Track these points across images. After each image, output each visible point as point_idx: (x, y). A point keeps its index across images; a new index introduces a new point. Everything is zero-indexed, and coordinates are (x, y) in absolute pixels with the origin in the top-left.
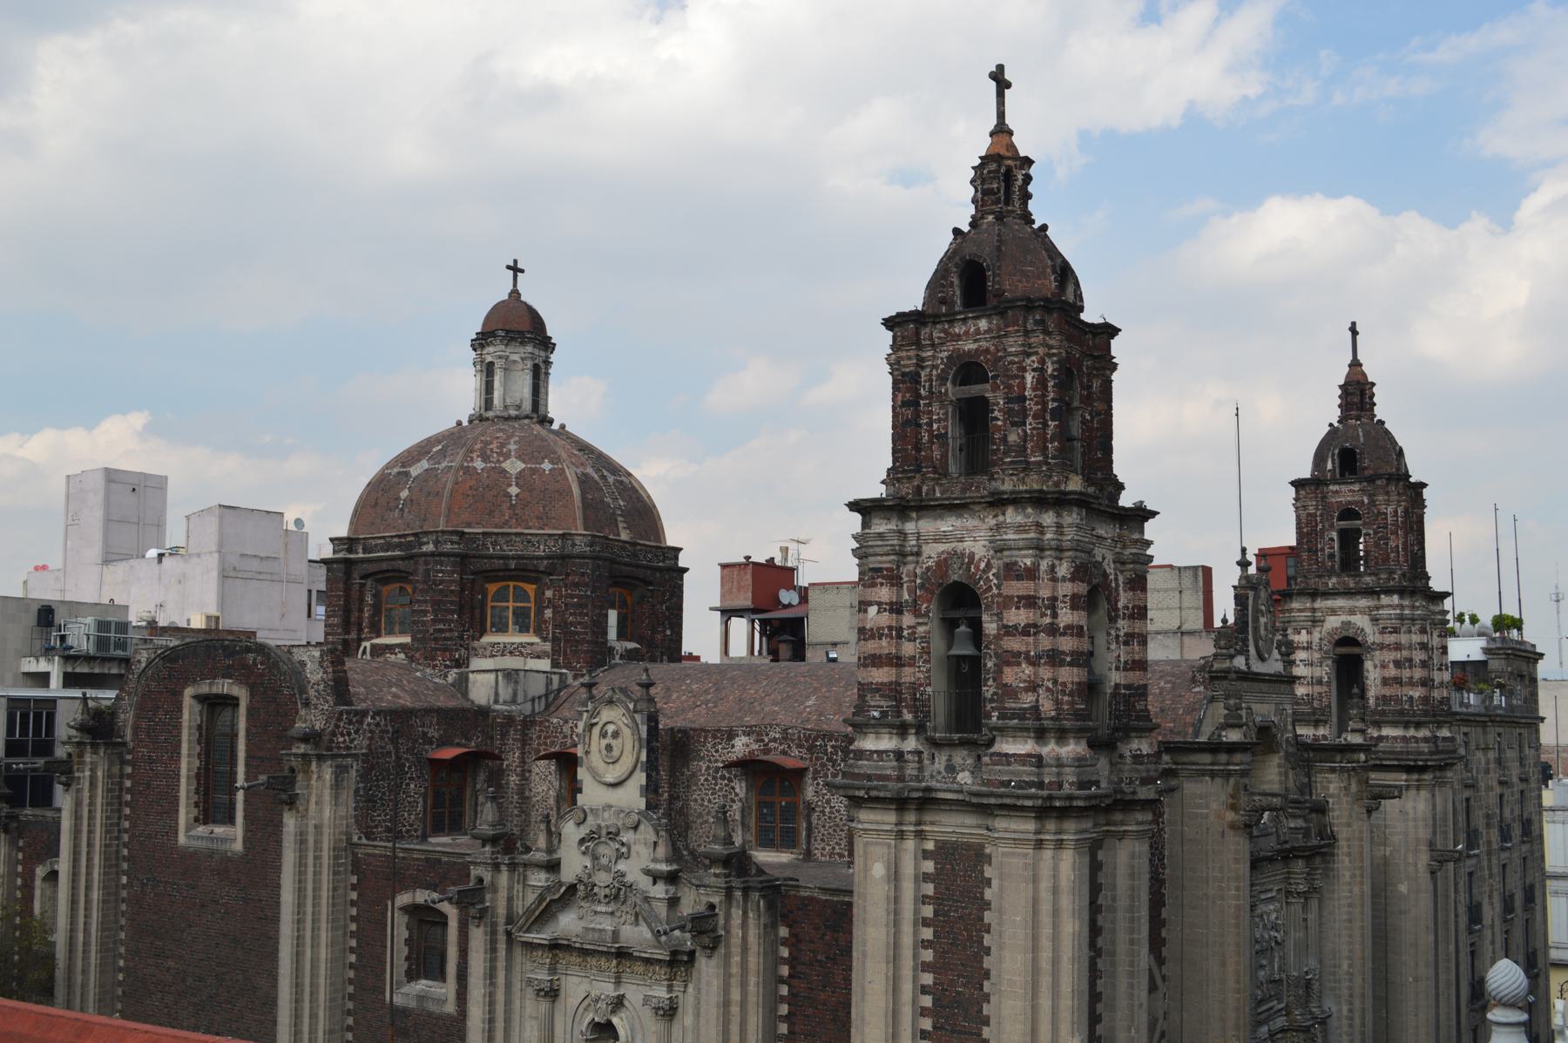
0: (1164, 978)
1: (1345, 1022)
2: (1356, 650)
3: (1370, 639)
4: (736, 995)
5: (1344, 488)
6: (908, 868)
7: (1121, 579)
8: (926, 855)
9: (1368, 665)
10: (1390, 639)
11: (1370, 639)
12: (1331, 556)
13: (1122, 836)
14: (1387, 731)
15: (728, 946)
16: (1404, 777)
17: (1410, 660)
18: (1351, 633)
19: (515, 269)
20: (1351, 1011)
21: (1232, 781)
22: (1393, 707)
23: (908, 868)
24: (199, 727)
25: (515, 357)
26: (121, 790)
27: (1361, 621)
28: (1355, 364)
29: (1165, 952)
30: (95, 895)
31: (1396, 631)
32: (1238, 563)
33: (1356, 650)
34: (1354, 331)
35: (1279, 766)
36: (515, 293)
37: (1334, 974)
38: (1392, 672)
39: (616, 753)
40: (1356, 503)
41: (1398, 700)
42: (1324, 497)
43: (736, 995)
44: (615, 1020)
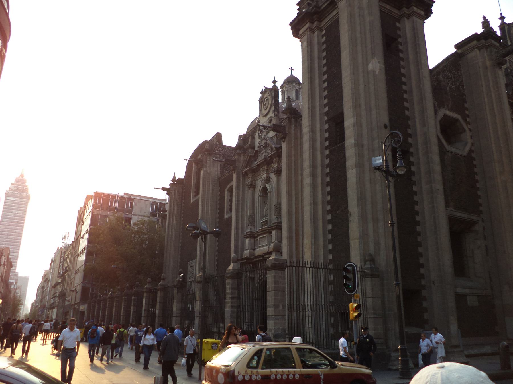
0: (470, 130)
4: (293, 153)
13: (409, 17)
19: (291, 69)
21: (489, 50)
24: (196, 172)
25: (291, 88)
29: (468, 120)
32: (500, 19)
36: (292, 74)
39: (267, 104)
43: (293, 153)
44: (267, 185)
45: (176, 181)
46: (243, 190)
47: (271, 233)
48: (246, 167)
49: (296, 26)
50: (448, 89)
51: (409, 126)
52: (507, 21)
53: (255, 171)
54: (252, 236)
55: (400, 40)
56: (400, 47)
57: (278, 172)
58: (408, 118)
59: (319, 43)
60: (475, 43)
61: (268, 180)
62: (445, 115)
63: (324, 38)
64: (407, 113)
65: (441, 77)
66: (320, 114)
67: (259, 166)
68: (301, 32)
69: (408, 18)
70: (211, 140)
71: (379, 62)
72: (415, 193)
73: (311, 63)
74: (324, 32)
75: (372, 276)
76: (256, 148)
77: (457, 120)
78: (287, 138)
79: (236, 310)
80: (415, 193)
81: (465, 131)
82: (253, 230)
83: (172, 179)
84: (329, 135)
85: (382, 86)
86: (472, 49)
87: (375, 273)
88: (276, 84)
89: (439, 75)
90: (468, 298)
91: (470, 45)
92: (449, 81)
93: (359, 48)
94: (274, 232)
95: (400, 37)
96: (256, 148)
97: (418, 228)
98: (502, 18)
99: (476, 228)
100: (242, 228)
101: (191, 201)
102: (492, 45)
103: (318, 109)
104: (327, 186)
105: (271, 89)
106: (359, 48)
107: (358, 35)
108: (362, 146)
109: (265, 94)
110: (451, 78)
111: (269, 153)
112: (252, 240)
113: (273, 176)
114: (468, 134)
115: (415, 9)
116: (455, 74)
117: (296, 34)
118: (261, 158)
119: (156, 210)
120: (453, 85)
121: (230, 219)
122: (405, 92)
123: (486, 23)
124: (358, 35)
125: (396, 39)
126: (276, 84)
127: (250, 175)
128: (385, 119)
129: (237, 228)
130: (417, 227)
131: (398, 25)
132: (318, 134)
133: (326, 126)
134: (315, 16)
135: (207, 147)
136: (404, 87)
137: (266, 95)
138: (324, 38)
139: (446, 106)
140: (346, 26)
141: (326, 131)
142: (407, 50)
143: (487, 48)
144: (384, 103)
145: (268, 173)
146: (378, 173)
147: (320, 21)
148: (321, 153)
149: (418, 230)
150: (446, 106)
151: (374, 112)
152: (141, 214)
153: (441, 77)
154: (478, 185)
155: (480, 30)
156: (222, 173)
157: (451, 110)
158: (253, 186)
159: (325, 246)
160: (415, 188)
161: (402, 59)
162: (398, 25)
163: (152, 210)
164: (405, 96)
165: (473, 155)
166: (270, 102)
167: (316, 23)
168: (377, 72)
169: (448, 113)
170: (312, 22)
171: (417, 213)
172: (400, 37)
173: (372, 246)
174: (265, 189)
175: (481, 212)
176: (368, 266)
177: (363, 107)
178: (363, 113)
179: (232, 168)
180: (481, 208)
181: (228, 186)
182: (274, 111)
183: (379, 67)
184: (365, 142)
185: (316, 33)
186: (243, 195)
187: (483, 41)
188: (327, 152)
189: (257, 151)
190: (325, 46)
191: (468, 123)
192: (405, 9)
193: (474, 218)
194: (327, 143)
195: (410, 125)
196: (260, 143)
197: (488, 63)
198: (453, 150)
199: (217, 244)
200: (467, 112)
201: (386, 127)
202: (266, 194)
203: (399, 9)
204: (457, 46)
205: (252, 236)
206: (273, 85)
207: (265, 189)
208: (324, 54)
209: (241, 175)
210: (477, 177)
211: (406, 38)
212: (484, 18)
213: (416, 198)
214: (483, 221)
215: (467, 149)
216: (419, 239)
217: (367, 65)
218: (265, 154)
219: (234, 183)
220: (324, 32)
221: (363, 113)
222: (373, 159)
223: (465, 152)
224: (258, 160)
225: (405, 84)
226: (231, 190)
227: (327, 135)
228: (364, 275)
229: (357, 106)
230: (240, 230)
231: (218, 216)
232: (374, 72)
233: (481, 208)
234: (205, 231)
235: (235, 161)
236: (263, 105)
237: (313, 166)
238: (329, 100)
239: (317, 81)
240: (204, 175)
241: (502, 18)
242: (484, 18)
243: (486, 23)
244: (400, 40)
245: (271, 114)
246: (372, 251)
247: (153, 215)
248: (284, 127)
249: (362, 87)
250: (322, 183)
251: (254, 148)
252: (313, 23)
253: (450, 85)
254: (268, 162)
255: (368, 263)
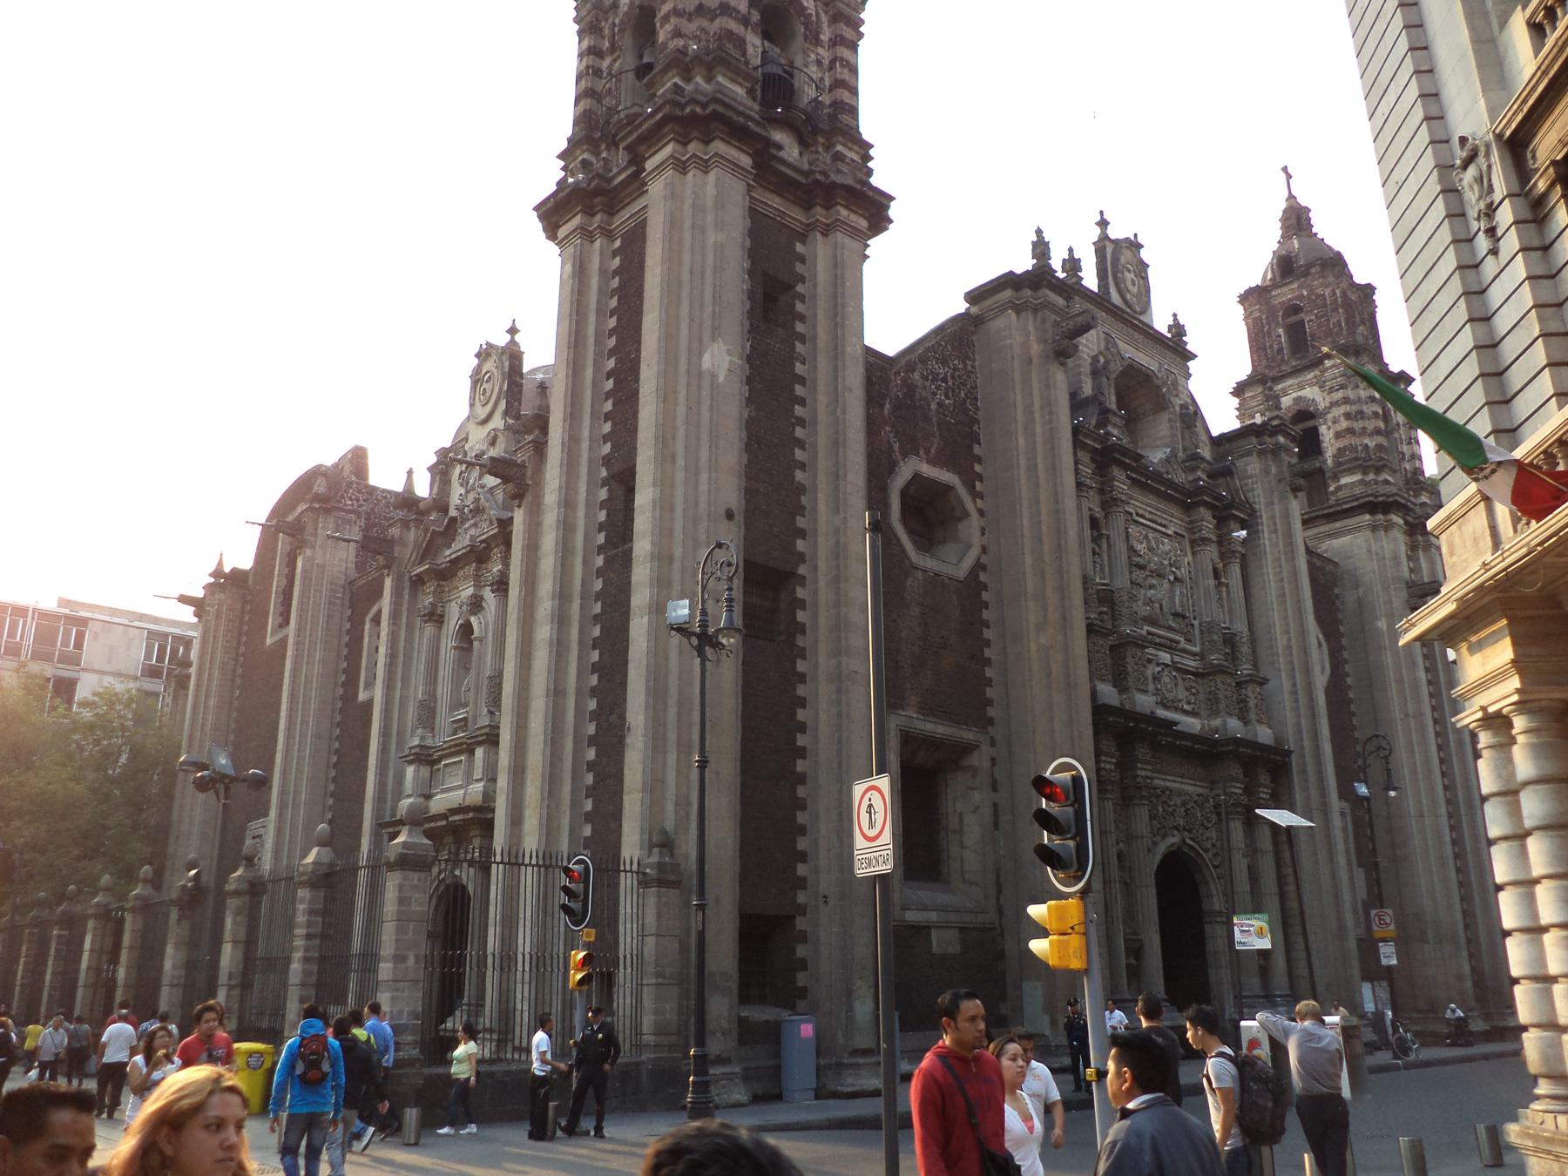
0: (981, 513)
1: (1286, 696)
2: (1309, 424)
3: (1322, 406)
5: (1285, 289)
6: (595, 264)
7: (824, 18)
8: (614, 254)
9: (1323, 429)
10: (1339, 395)
11: (1322, 406)
12: (1280, 350)
13: (827, 231)
14: (1344, 481)
15: (539, 498)
16: (1368, 517)
17: (1361, 412)
18: (1302, 406)
20: (1295, 685)
21: (1039, 315)
22: (1349, 455)
23: (595, 264)
26: (241, 622)
27: (1311, 393)
28: (1291, 197)
30: (212, 702)
31: (1343, 387)
33: (1309, 424)
34: (1285, 169)
35: (1170, 421)
37: (1271, 647)
38: (1344, 424)
40: (1297, 298)
41: (1353, 449)
42: (1268, 303)
44: (472, 619)
45: (225, 576)
46: (410, 627)
47: (472, 752)
48: (420, 563)
49: (552, 214)
50: (934, 406)
51: (801, 510)
52: (1114, 233)
53: (445, 575)
54: (426, 758)
55: (800, 288)
56: (799, 307)
57: (501, 586)
58: (802, 489)
59: (602, 272)
60: (1008, 294)
61: (476, 605)
62: (917, 476)
63: (617, 260)
64: (799, 476)
65: (917, 376)
66: (590, 460)
67: (456, 563)
68: (562, 233)
69: (825, 235)
70: (336, 466)
71: (729, 352)
72: (802, 678)
73: (577, 323)
74: (618, 243)
75: (661, 883)
76: (453, 513)
77: (948, 488)
78: (528, 498)
79: (315, 968)
80: (802, 678)
81: (967, 515)
82: (429, 742)
83: (212, 568)
84: (608, 515)
85: (731, 413)
86: (1002, 309)
87: (663, 878)
88: (517, 338)
89: (913, 370)
90: (934, 934)
91: (996, 298)
92: (938, 387)
93: (685, 309)
94: (479, 752)
95: (802, 279)
96: (453, 513)
97: (801, 766)
98: (1103, 223)
99: (975, 759)
100: (400, 734)
101: (269, 641)
102: (1046, 305)
103: (585, 445)
104: (594, 647)
105: (504, 350)
106: (685, 309)
107: (686, 276)
108: (671, 560)
109: (485, 360)
110: (944, 380)
111: (487, 530)
112: (425, 771)
113: (488, 594)
114: (975, 522)
115: (844, 212)
116: (956, 369)
117: (551, 231)
118: (461, 543)
119: (160, 658)
120: (947, 397)
121: (369, 704)
122: (802, 422)
123: (1041, 248)
124: (686, 276)
125: (792, 287)
126: (517, 338)
127: (430, 587)
128: (731, 494)
129: (385, 734)
130: (799, 762)
131: (799, 248)
132: (581, 513)
133: (603, 494)
134: (597, 200)
135: (320, 487)
136: (799, 411)
137: (489, 365)
138: (617, 260)
139: (922, 452)
140: (659, 250)
141: (602, 505)
142: (815, 315)
143: (1035, 310)
144: (732, 456)
145: (478, 586)
146: (676, 639)
147: (611, 211)
148: (585, 563)
149: (799, 769)
150: (922, 452)
151: (704, 477)
152: (108, 668)
153: (917, 376)
154: (987, 653)
155: (1023, 263)
156: (360, 566)
157: (932, 462)
158: (436, 617)
159: (574, 804)
160: (801, 666)
161: (802, 338)
162: (799, 248)
163: (148, 656)
164: (799, 432)
165: (983, 577)
166: (497, 385)
167: (598, 217)
168: (721, 379)
169: (927, 470)
170: (590, 212)
171: (802, 728)
172: (802, 279)
173: (670, 808)
174: (466, 630)
175: (990, 721)
176: (654, 859)
177: (681, 462)
178: (680, 477)
179: (381, 560)
180: (991, 712)
181: (374, 609)
182: (506, 413)
183: (726, 365)
184: (678, 551)
185: (598, 243)
186: (409, 640)
187: (1028, 292)
188: (600, 561)
189: (453, 520)
190: (616, 282)
191: (976, 495)
192: (818, 209)
193: (968, 735)
194: (601, 539)
195: (804, 508)
196: (463, 498)
197: (1035, 348)
198: (929, 563)
199: (333, 773)
200: (977, 468)
201: (730, 515)
202: (471, 642)
203: (808, 207)
204: (974, 297)
205: (426, 758)
206: (508, 337)
207: (466, 630)
208: (614, 303)
209: (407, 584)
210: (988, 634)
211: (815, 286)
212: (1039, 232)
213: (801, 691)
214: (993, 743)
215: (968, 563)
216: (801, 792)
217: (700, 355)
218: (472, 532)
219: (386, 603)
220: (618, 243)
221: (680, 477)
222: (671, 605)
223: (962, 570)
224: (455, 547)
225: (802, 402)
226: (377, 620)
227: (602, 516)
228: (644, 881)
229: (665, 457)
230: (394, 740)
231: (340, 691)
232: (714, 376)
233: (991, 712)
234: (225, 776)
235: (390, 543)
236: (479, 390)
237: (563, 596)
238: (614, 425)
239: (589, 372)
240: (304, 571)
241: (1103, 223)
242: (1039, 232)
243: (1041, 248)
244: (800, 288)
245: (497, 422)
246: (669, 824)
247: (152, 672)
248: (523, 466)
249: (681, 410)
250: (581, 642)
251: (445, 510)
252: (593, 215)
253: (940, 396)
254: (479, 555)
255: (656, 850)
